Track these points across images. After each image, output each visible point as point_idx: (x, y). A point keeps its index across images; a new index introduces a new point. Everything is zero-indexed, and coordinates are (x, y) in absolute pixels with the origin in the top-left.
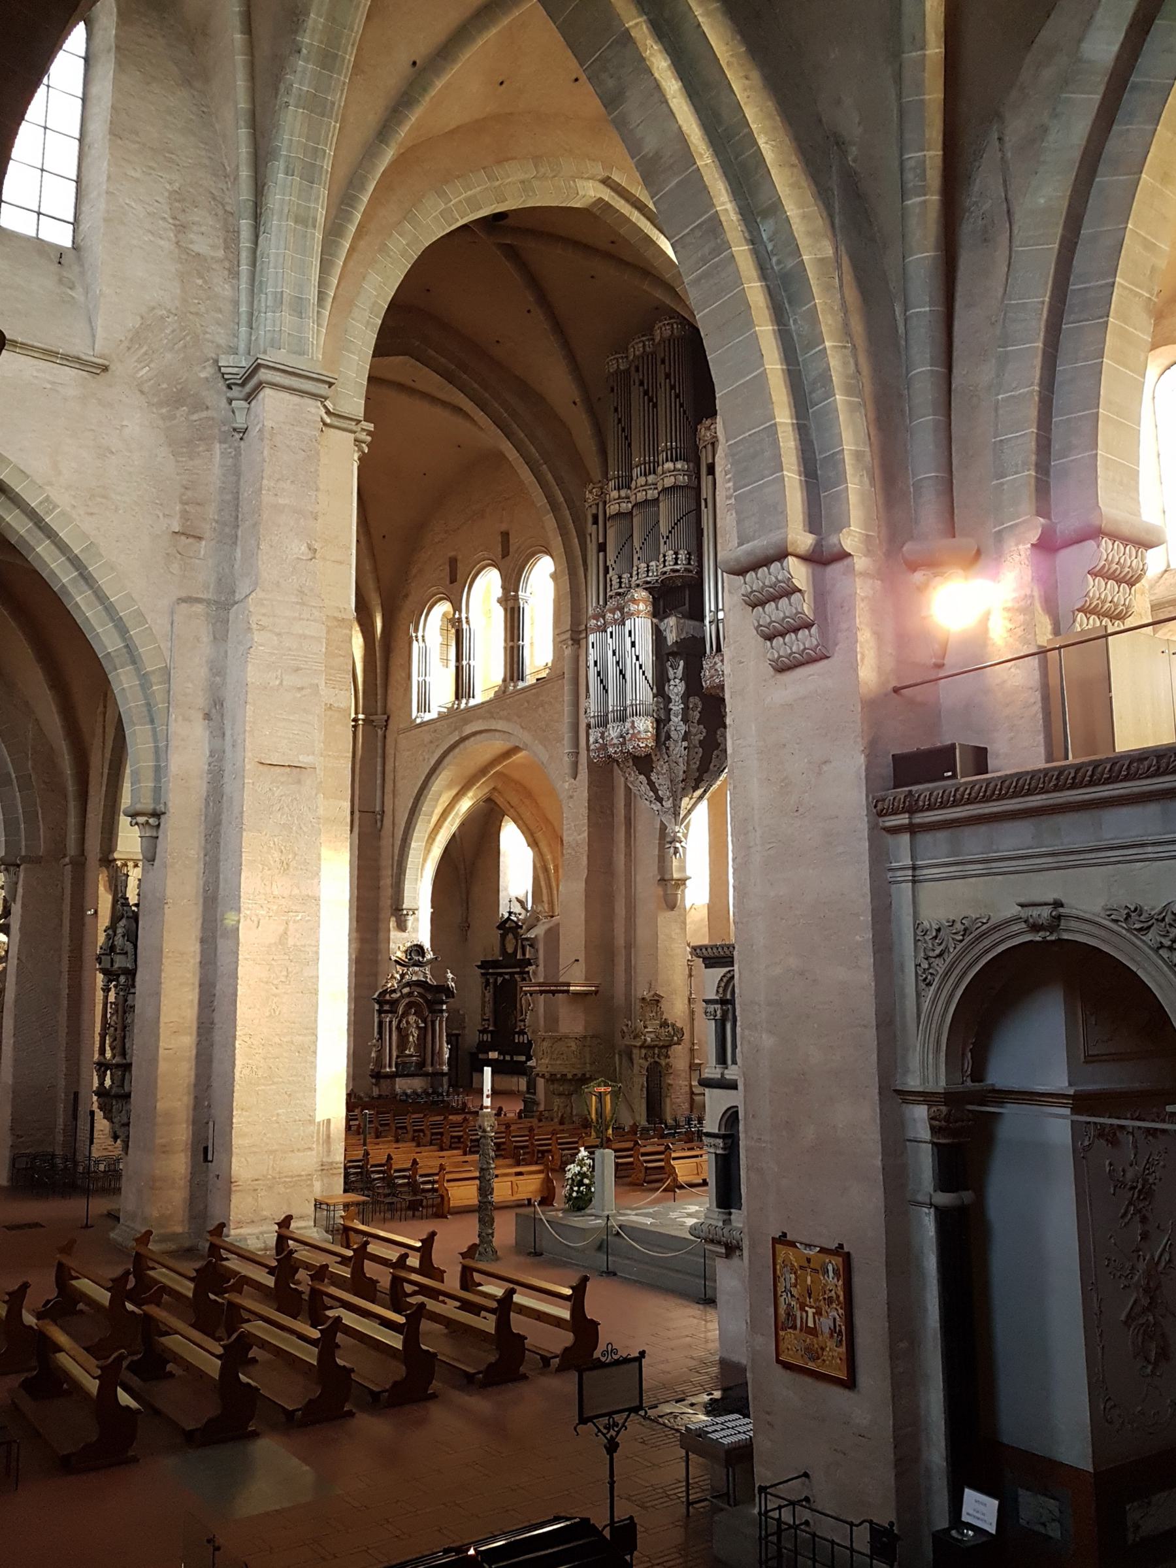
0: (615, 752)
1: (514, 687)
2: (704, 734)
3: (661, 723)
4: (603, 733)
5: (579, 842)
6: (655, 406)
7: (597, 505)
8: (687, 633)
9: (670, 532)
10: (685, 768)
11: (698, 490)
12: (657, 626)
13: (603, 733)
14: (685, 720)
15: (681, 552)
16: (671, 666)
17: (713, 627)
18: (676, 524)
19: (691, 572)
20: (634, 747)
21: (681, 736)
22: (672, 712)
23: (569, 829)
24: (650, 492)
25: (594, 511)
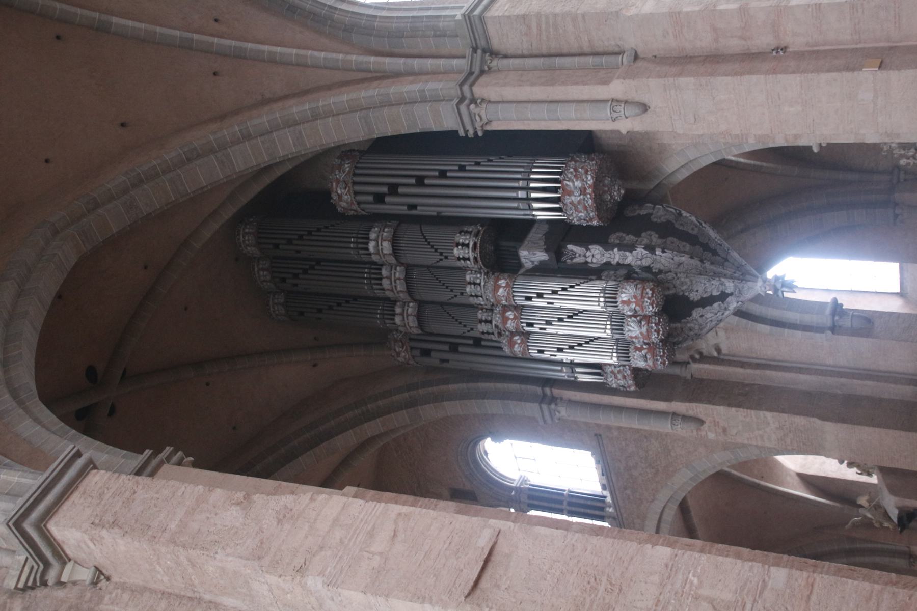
0: (658, 331)
1: (610, 507)
2: (653, 233)
3: (629, 274)
6: (318, 262)
8: (540, 240)
9: (436, 250)
10: (686, 255)
13: (637, 349)
14: (631, 248)
16: (572, 259)
17: (536, 205)
18: (429, 244)
19: (479, 232)
20: (652, 304)
21: (650, 255)
22: (621, 262)
23: (762, 437)
24: (397, 275)
25: (417, 353)
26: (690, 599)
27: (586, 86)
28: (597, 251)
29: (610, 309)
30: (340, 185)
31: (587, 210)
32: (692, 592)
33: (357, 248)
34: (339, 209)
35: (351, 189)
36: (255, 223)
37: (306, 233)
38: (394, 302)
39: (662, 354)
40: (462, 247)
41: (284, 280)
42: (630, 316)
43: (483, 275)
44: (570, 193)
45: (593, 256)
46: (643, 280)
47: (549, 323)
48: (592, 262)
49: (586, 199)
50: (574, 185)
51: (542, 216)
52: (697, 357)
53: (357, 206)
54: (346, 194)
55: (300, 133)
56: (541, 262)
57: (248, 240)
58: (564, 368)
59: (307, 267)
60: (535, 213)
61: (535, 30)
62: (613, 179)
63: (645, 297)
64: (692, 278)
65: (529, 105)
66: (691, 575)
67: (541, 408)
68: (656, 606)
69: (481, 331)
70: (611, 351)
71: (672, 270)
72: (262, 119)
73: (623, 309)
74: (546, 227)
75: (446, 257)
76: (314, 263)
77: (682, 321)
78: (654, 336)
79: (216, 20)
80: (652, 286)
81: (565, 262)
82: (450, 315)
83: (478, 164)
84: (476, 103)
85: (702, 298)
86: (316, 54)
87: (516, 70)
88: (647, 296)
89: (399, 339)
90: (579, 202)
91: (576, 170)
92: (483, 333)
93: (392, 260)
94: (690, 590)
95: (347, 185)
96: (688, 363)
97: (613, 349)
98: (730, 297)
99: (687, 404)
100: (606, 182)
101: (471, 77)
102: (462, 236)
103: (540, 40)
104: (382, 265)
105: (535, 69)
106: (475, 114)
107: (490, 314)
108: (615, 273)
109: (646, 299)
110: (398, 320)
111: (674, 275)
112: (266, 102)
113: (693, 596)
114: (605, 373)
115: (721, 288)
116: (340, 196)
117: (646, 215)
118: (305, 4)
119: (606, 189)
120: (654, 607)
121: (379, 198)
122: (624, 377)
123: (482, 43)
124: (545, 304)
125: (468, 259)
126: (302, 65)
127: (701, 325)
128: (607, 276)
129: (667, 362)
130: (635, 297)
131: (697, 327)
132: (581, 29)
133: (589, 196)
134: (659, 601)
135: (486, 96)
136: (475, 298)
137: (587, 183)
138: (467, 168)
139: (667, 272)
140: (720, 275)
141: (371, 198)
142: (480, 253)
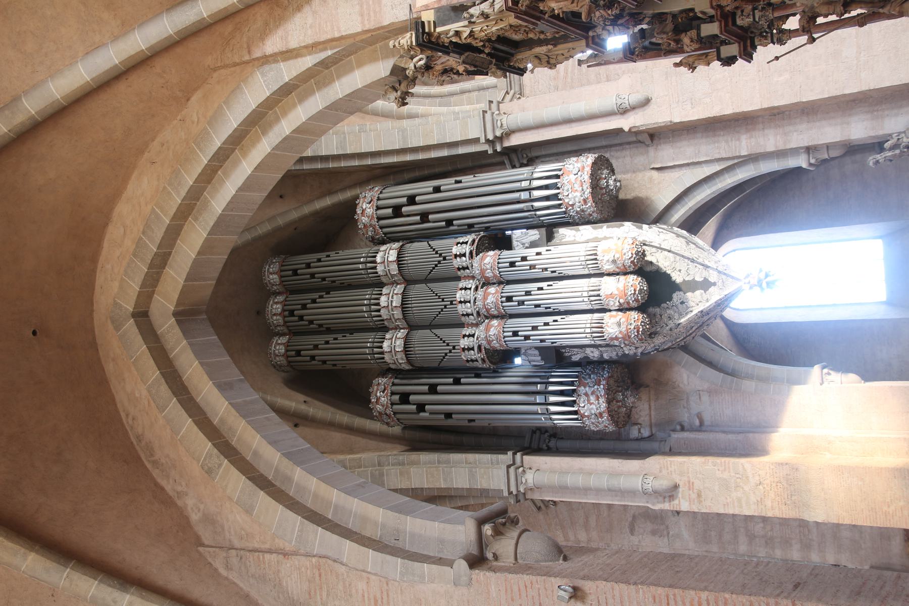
23: (739, 500)
35: (375, 202)
52: (678, 427)
53: (376, 220)
54: (370, 208)
67: (508, 472)
77: (662, 305)
85: (684, 280)
98: (713, 287)
106: (497, 120)
119: (604, 176)
122: (598, 398)
127: (681, 315)
131: (676, 316)
133: (586, 173)
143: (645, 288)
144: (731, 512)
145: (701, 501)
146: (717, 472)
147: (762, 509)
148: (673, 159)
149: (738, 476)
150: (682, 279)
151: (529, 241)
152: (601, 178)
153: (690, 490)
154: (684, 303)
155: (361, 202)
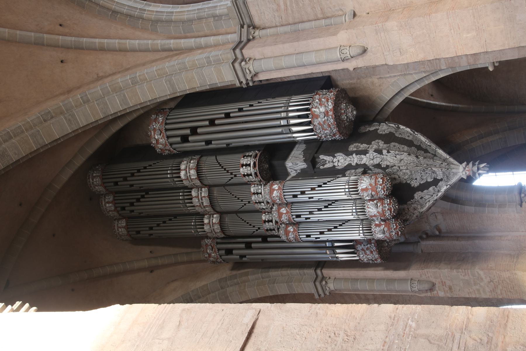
2: (380, 141)
4: (376, 225)
5: (488, 279)
6: (147, 191)
7: (219, 250)
9: (228, 172)
10: (405, 153)
11: (201, 153)
12: (293, 177)
13: (376, 225)
14: (365, 152)
15: (242, 162)
16: (323, 165)
17: (294, 129)
18: (222, 167)
19: (256, 155)
21: (379, 155)
23: (478, 290)
26: (410, 337)
27: (322, 39)
28: (341, 157)
29: (354, 197)
30: (156, 132)
31: (330, 127)
32: (411, 333)
33: (173, 177)
34: (157, 151)
36: (100, 169)
37: (136, 171)
38: (201, 216)
39: (395, 227)
40: (246, 167)
41: (123, 208)
42: (370, 200)
43: (263, 186)
44: (317, 117)
45: (338, 161)
46: (376, 174)
47: (311, 213)
48: (338, 165)
49: (329, 119)
50: (320, 110)
51: (300, 137)
52: (424, 236)
54: (162, 139)
55: (124, 96)
56: (302, 170)
57: (96, 181)
58: (328, 251)
59: (140, 197)
60: (294, 135)
61: (282, 7)
62: (347, 104)
63: (378, 184)
64: (411, 169)
65: (283, 58)
66: (410, 321)
67: (315, 285)
68: (384, 346)
69: (266, 229)
70: (358, 229)
71: (396, 164)
72: (97, 89)
73: (363, 196)
74: (303, 146)
75: (235, 176)
76: (144, 193)
77: (408, 203)
78: (387, 214)
79: (61, 25)
80: (382, 176)
81: (319, 168)
82: (243, 220)
83: (251, 106)
84: (246, 61)
85: (420, 184)
86: (133, 42)
87: (272, 35)
88: (379, 184)
89: (209, 244)
90: (324, 122)
91: (320, 100)
92: (267, 230)
93: (198, 183)
94: (410, 331)
95: (161, 132)
96: (419, 242)
97: (359, 228)
98: (440, 182)
99: (421, 271)
100: (342, 106)
101: (240, 45)
102: (245, 159)
103: (287, 14)
104: (192, 189)
105: (285, 33)
106: (245, 69)
107: (271, 215)
108: (355, 171)
109: (379, 186)
110: (206, 228)
111: (398, 168)
112: (99, 78)
113: (412, 335)
114: (358, 251)
115: (434, 175)
116: (157, 141)
117: (374, 130)
118: (123, 9)
119: (343, 111)
120: (382, 347)
121: (185, 139)
122: (372, 252)
123: (247, 21)
124: (307, 199)
125: (251, 175)
126: (123, 50)
127: (422, 205)
128: (349, 174)
129: (400, 233)
130: (370, 185)
131: (419, 207)
132: (315, 2)
133: (331, 117)
134: (385, 342)
135: (251, 55)
136: (259, 204)
137: (328, 108)
138: (244, 109)
139: (393, 167)
140: (432, 166)
141: (179, 139)
142: (258, 169)
143: (394, 199)
144: (474, 296)
145: (453, 292)
146: (460, 276)
147: (494, 294)
148: (389, 72)
149: (475, 278)
150: (419, 184)
151: (300, 169)
152: (341, 114)
153: (443, 285)
154: (423, 198)
155: (153, 134)
